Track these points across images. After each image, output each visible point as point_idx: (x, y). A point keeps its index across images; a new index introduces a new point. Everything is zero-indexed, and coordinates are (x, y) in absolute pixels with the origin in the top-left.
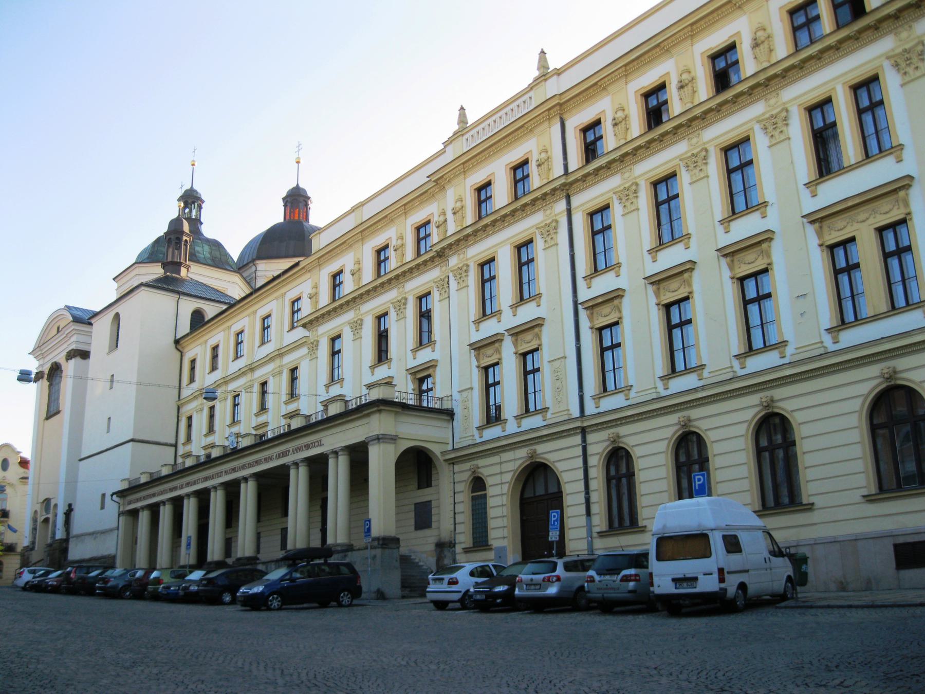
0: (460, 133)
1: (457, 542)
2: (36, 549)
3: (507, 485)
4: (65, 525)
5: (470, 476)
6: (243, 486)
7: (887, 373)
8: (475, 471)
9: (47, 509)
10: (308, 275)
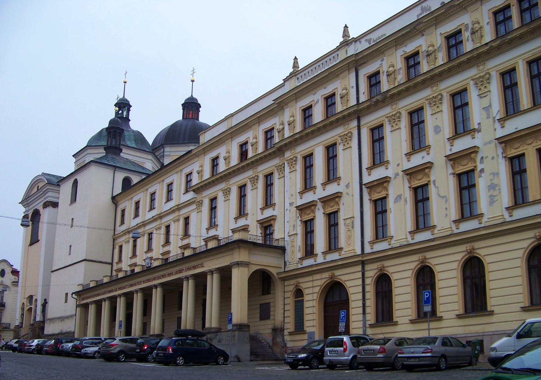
0: (294, 74)
1: (285, 328)
2: (23, 327)
4: (42, 313)
6: (154, 290)
7: (538, 235)
8: (297, 285)
9: (31, 303)
10: (197, 159)
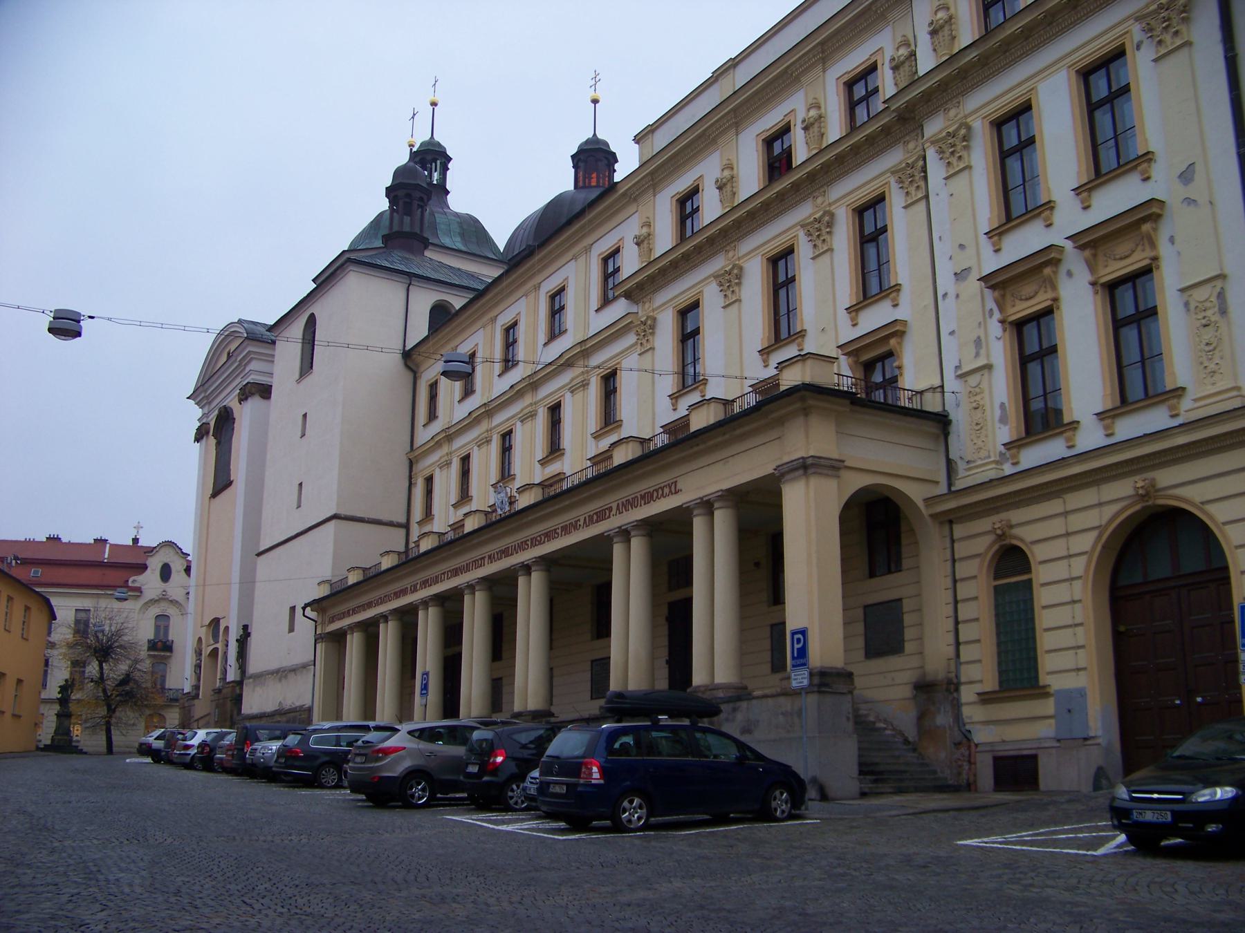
1: (963, 679)
3: (1084, 559)
6: (522, 581)
8: (1004, 534)
9: (215, 637)
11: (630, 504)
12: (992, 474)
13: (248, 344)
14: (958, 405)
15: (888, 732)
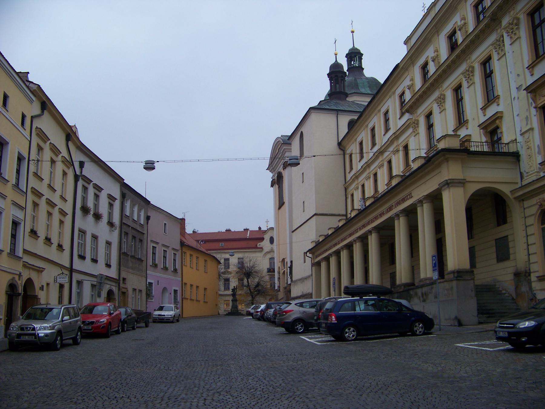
5: (538, 210)
11: (398, 203)
12: (535, 178)
13: (283, 146)
14: (522, 147)
15: (506, 295)
